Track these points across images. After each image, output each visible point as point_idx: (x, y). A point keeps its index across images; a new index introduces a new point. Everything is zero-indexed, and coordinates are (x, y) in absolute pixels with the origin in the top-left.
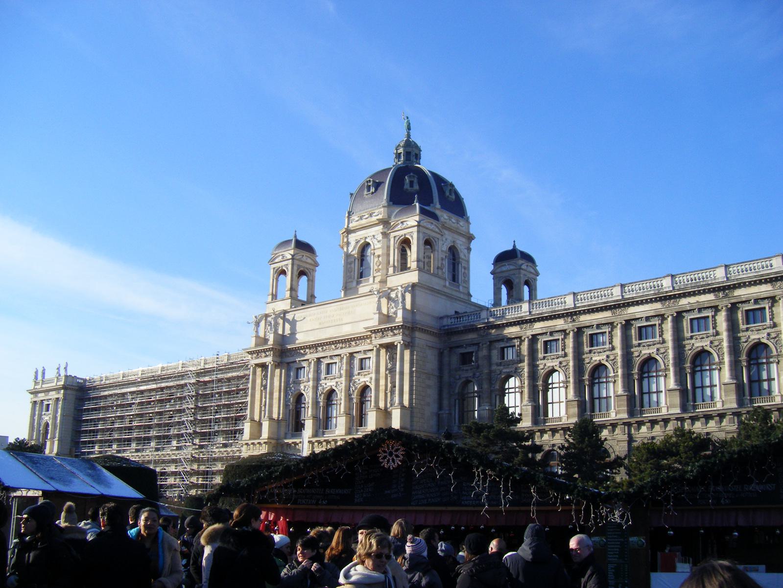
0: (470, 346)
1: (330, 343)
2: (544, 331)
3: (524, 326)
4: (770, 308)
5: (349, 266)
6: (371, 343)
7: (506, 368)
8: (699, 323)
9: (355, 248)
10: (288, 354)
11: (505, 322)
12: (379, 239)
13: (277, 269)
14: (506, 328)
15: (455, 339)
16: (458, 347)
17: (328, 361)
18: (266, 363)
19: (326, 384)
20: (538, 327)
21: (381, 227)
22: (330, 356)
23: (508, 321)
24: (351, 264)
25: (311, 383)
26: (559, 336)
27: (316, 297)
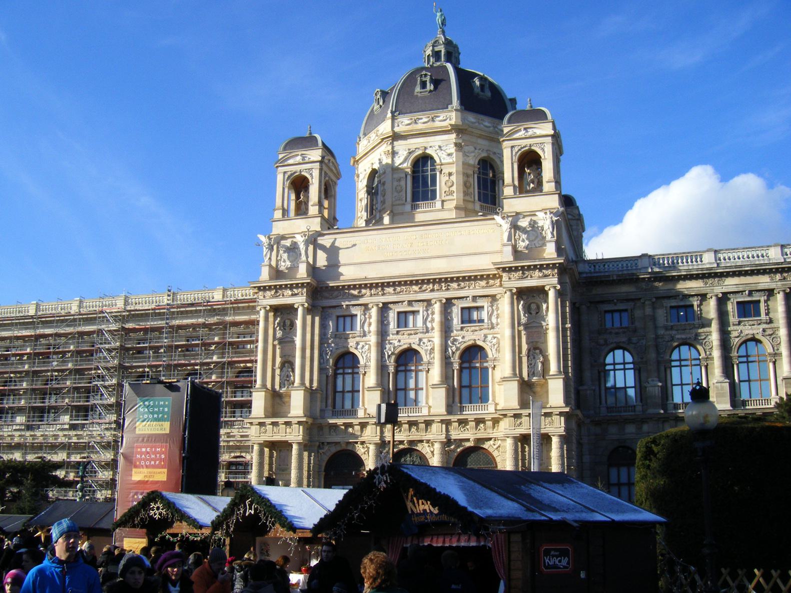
0: (621, 302)
1: (412, 283)
2: (741, 289)
3: (710, 281)
4: (766, 302)
5: (395, 183)
6: (501, 286)
7: (681, 334)
8: (748, 309)
9: (405, 160)
10: (326, 294)
11: (685, 273)
12: (449, 152)
13: (292, 175)
14: (681, 282)
15: (598, 291)
16: (603, 302)
17: (404, 308)
18: (294, 304)
19: (399, 341)
20: (731, 283)
21: (454, 136)
22: (409, 301)
23: (689, 273)
24: (399, 180)
25: (373, 339)
26: (761, 296)
27: (337, 221)
